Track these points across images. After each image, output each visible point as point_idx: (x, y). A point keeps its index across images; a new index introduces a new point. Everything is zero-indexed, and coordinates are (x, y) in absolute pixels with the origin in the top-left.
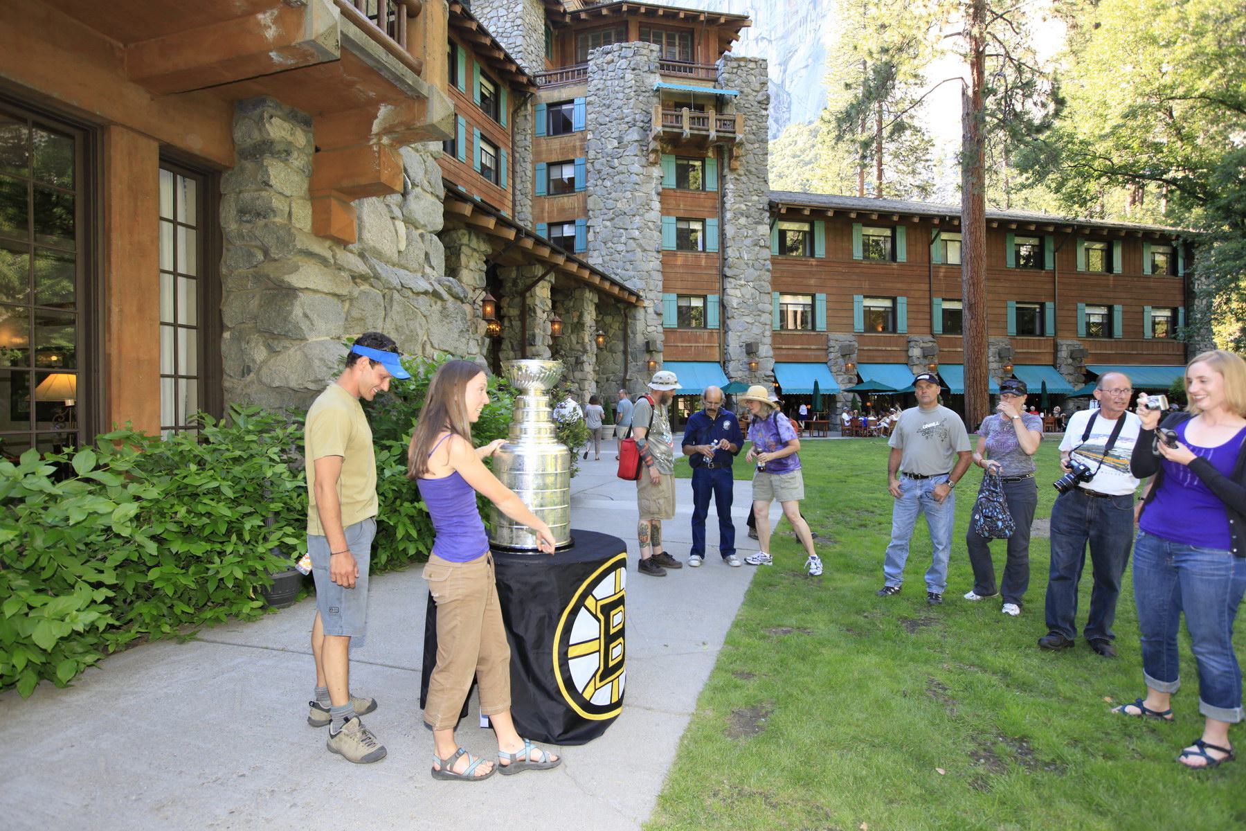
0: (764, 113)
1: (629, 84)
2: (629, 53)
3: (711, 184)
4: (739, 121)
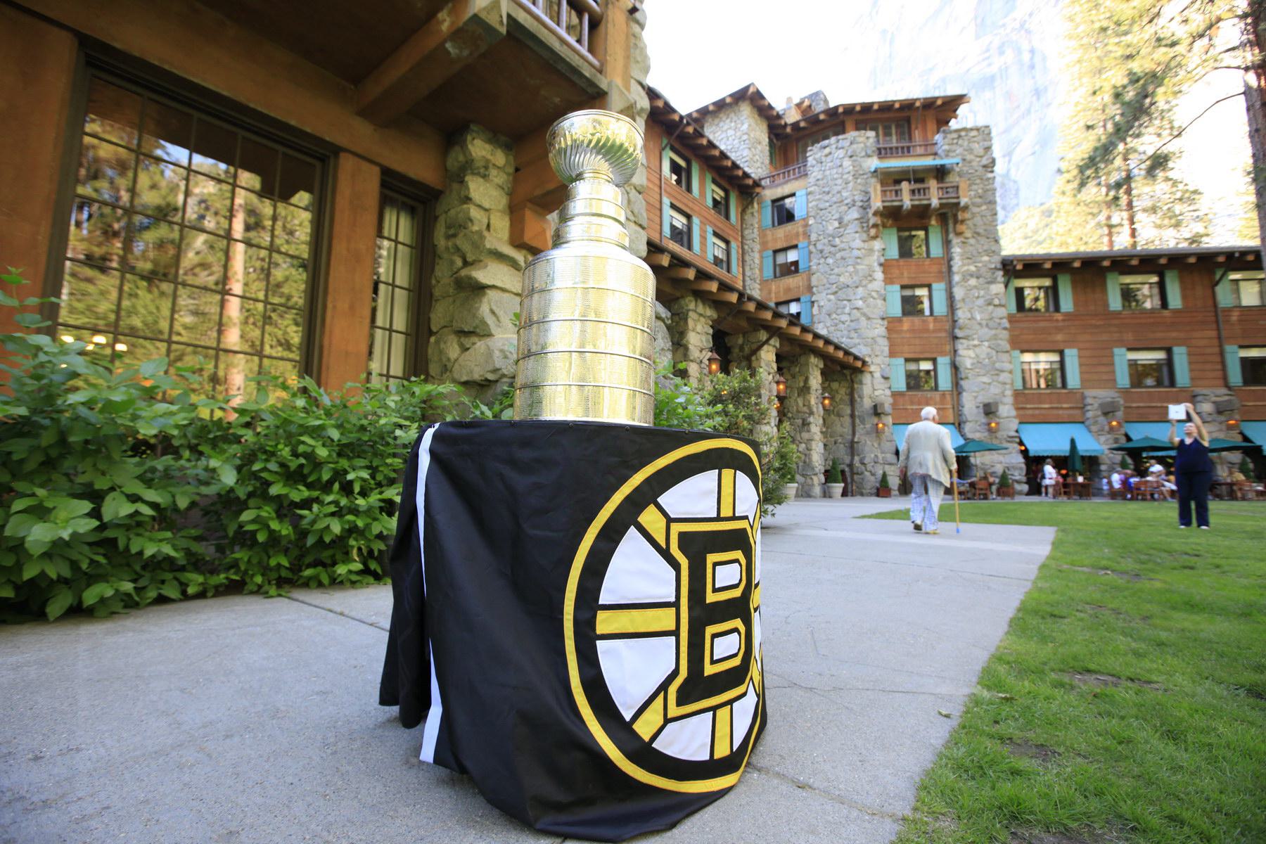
0: (990, 175)
1: (847, 171)
2: (846, 143)
3: (936, 250)
4: (963, 186)
